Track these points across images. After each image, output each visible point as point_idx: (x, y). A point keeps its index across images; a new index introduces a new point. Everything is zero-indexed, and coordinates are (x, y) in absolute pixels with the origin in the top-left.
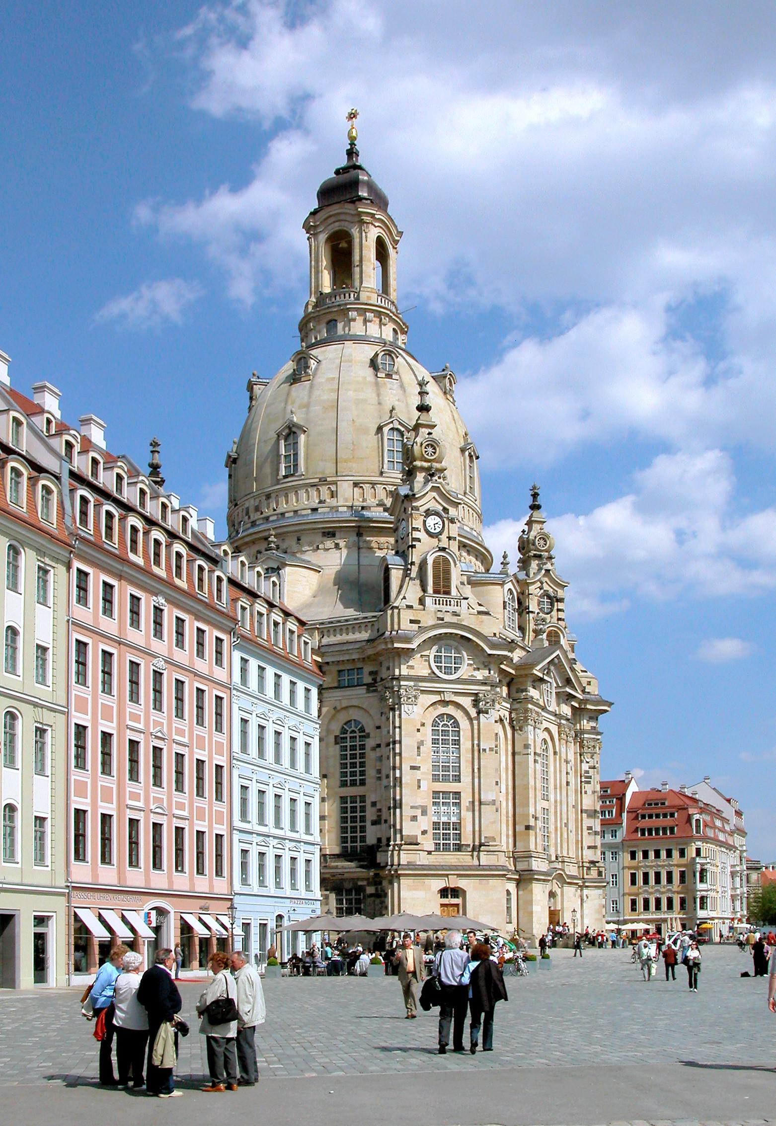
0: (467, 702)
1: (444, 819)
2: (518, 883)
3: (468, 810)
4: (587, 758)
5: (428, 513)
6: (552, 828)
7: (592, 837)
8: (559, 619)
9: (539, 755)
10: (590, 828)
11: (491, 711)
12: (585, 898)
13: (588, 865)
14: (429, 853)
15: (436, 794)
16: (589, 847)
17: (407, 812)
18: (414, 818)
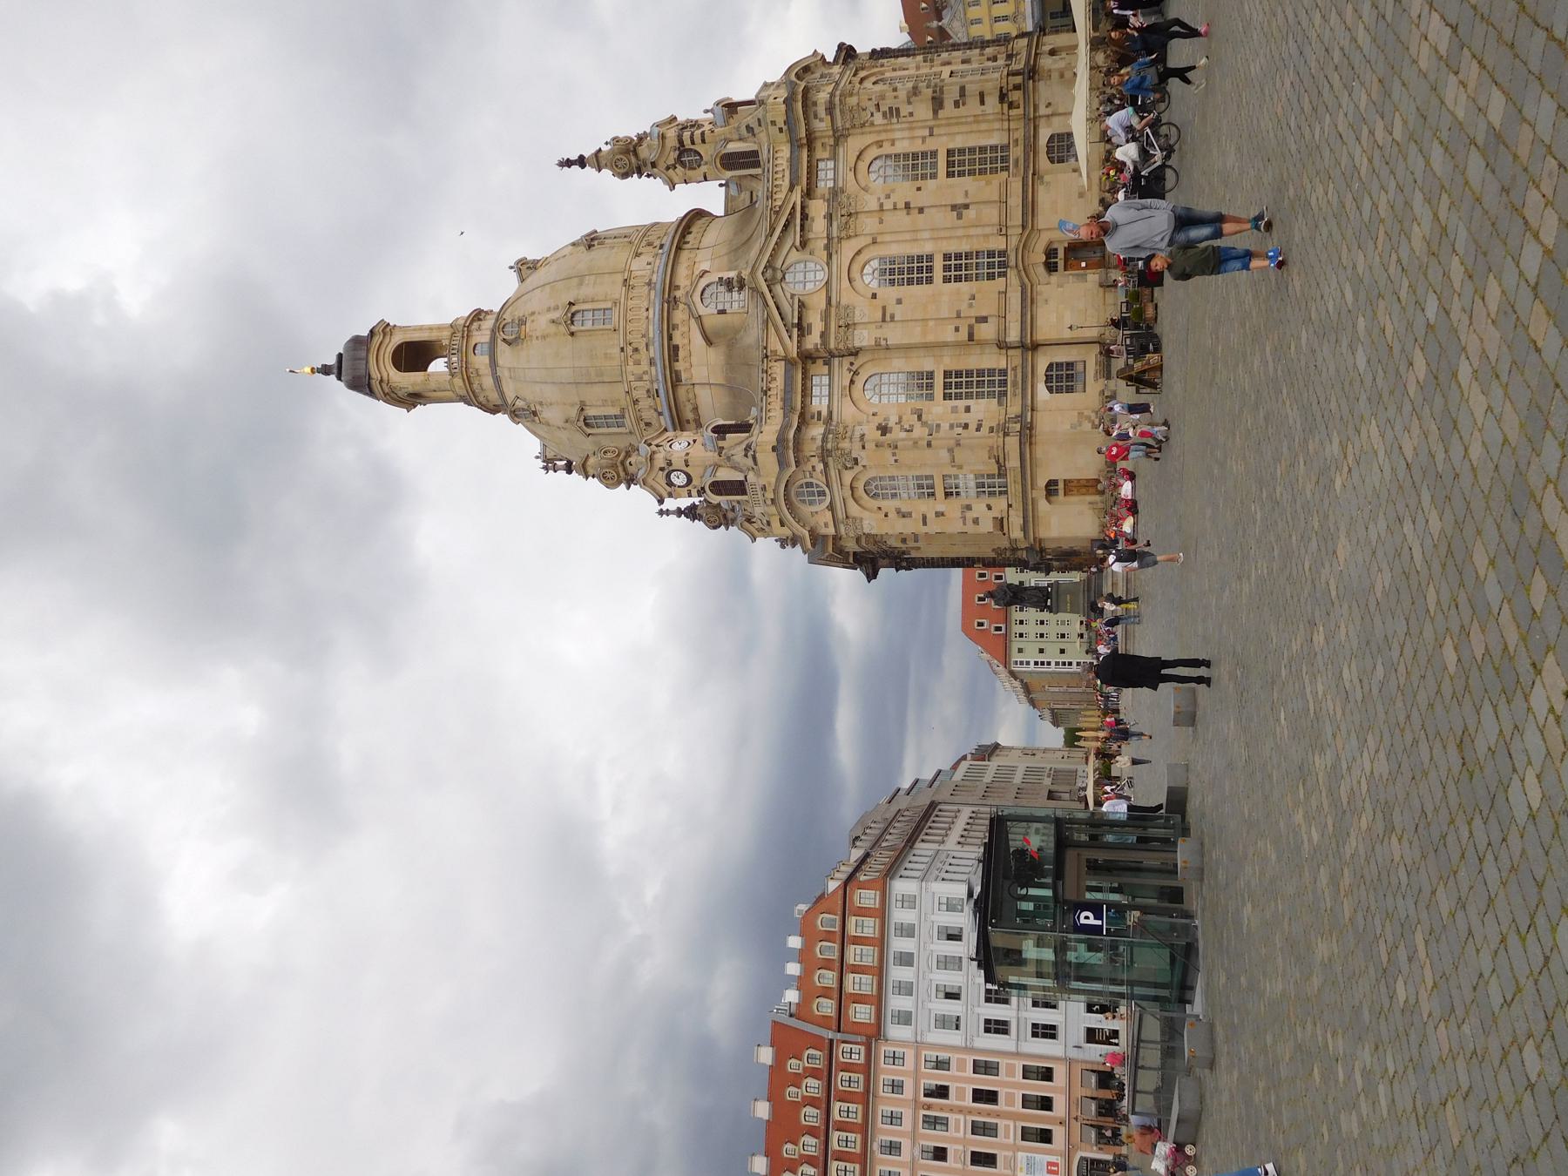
0: (848, 477)
1: (972, 484)
2: (1035, 347)
3: (960, 467)
4: (866, 116)
5: (670, 484)
6: (964, 247)
7: (968, 100)
8: (703, 141)
9: (884, 308)
10: (957, 104)
11: (854, 455)
12: (1049, 111)
13: (1006, 106)
14: (1010, 506)
15: (948, 495)
16: (982, 102)
17: (970, 528)
18: (976, 521)
